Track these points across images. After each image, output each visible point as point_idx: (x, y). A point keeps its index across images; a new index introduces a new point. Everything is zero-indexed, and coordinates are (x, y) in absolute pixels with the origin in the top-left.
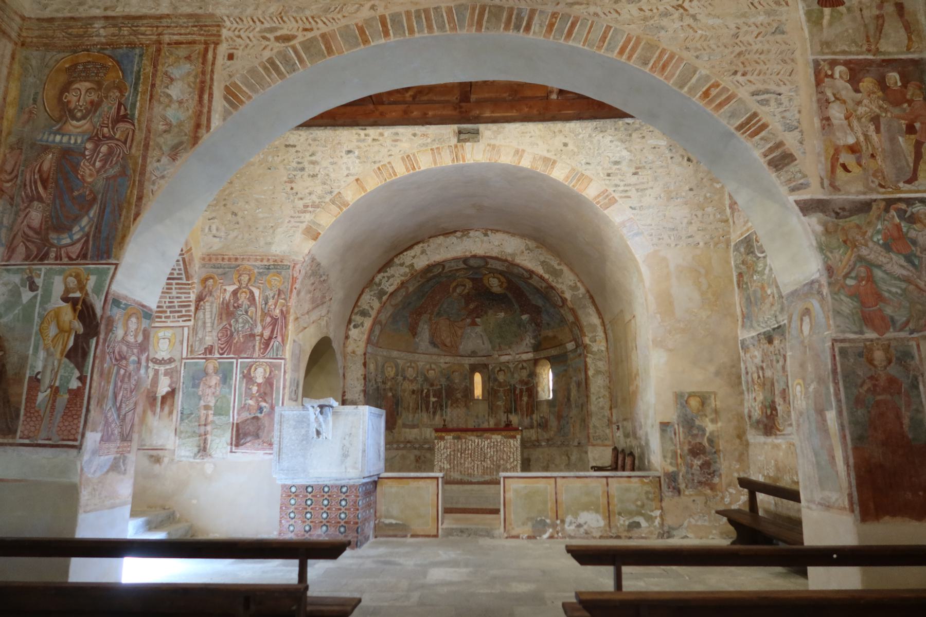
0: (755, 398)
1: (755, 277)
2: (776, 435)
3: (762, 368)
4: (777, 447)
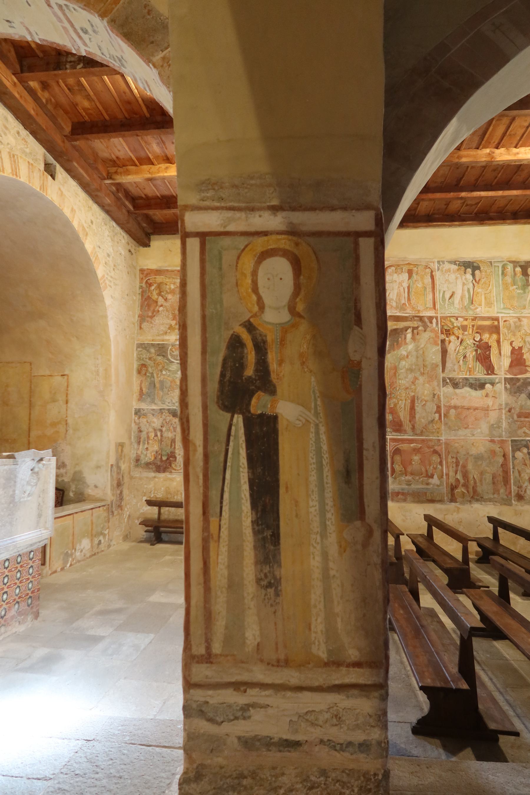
0: (147, 448)
1: (164, 372)
2: (171, 472)
3: (161, 431)
4: (172, 480)
